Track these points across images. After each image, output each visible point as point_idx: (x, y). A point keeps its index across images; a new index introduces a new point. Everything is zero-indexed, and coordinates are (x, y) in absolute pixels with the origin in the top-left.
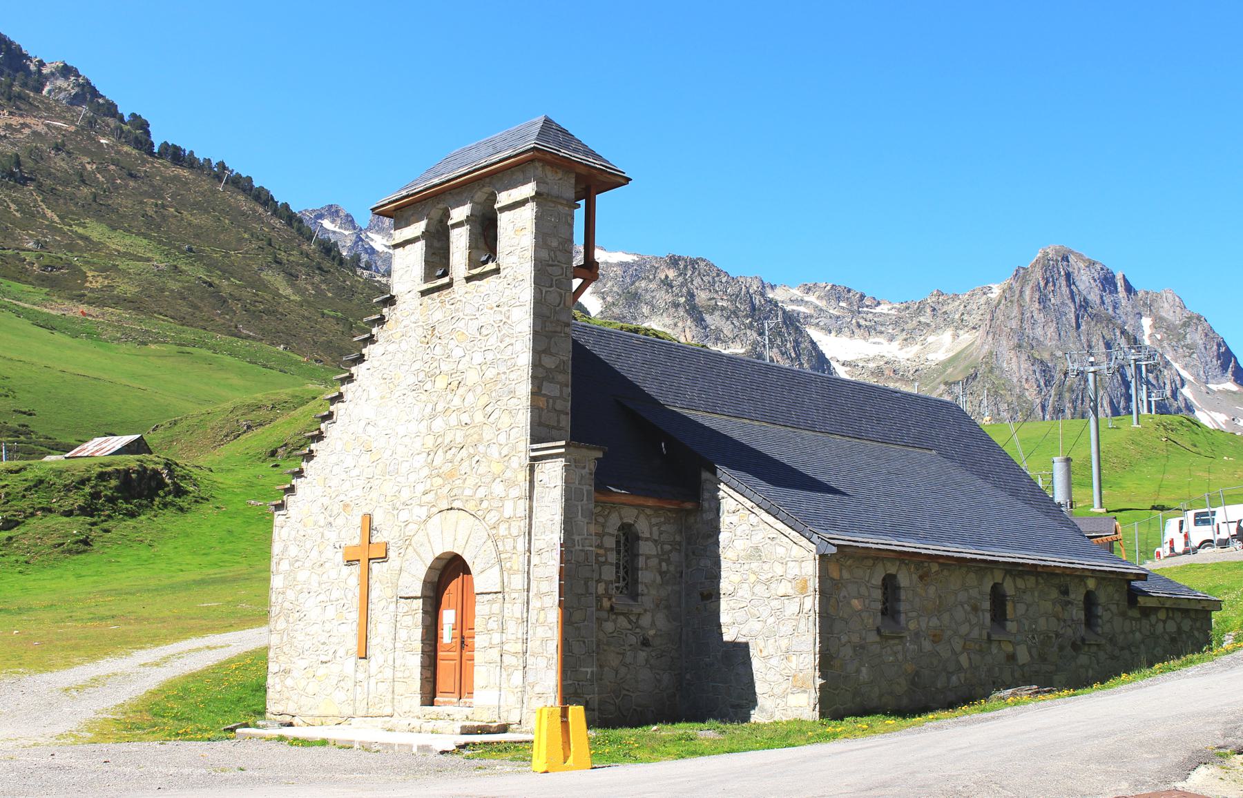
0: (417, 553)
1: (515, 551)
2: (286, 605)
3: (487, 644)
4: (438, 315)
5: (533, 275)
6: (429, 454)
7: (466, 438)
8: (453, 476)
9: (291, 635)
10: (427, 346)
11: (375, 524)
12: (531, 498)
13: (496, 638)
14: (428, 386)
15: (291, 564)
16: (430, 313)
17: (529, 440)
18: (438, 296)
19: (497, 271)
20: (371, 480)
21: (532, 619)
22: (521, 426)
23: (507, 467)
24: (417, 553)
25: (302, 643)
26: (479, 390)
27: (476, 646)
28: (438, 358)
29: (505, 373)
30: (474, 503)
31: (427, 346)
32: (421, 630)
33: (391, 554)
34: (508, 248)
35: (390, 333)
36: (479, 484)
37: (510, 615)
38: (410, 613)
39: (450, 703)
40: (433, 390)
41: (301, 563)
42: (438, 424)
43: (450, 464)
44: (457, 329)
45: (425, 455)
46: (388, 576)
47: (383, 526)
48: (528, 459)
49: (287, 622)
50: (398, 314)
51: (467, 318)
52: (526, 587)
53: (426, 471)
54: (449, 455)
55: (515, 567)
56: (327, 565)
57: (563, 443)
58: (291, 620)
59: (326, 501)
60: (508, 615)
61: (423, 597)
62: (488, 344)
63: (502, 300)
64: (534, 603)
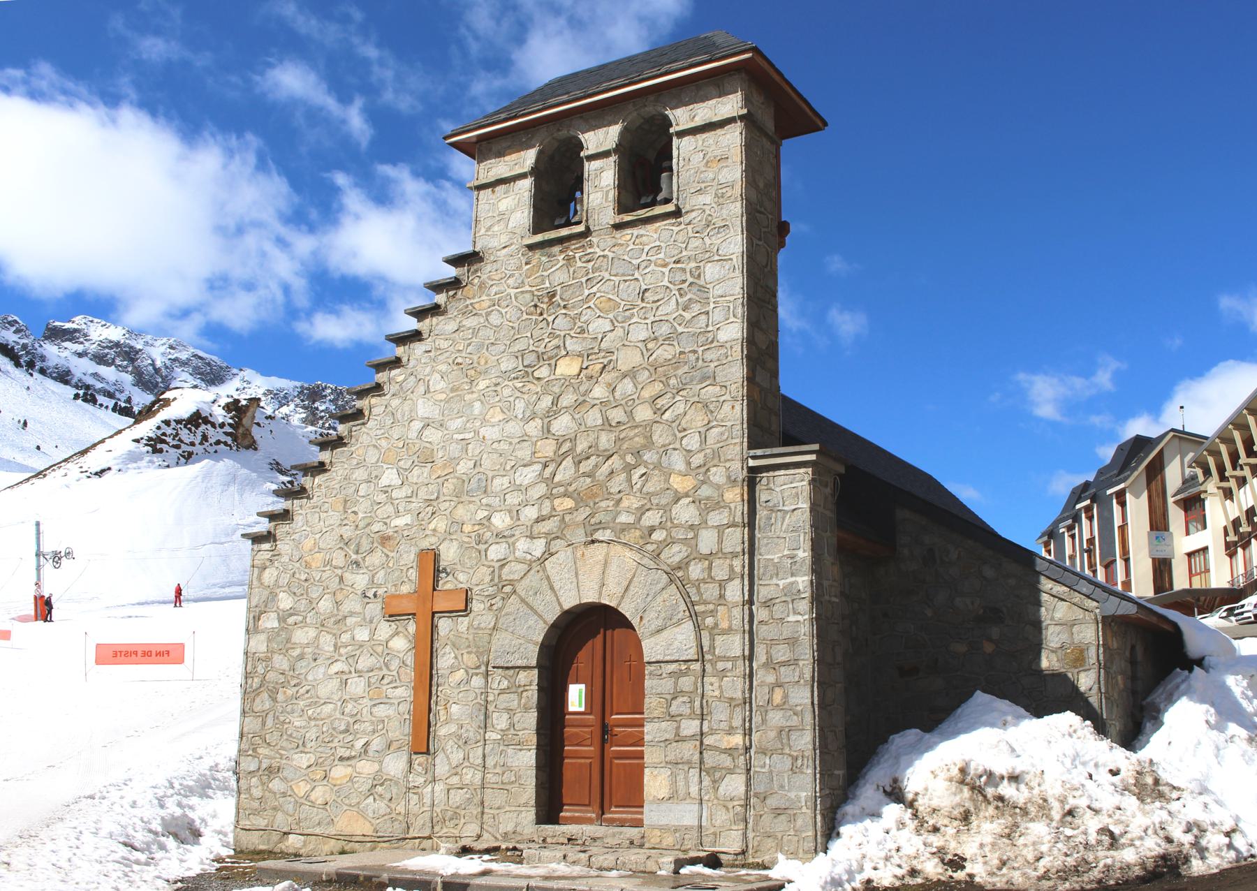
0: (527, 604)
1: (722, 601)
2: (271, 676)
3: (670, 736)
4: (560, 276)
5: (744, 218)
6: (545, 466)
7: (618, 443)
8: (594, 495)
9: (282, 719)
10: (541, 318)
11: (443, 564)
12: (751, 524)
13: (690, 727)
14: (543, 372)
15: (282, 619)
16: (545, 274)
17: (745, 444)
18: (561, 252)
19: (677, 213)
20: (435, 503)
21: (760, 696)
22: (729, 424)
23: (703, 482)
24: (527, 604)
25: (303, 731)
26: (643, 376)
27: (647, 738)
28: (562, 334)
29: (695, 352)
30: (638, 533)
31: (541, 318)
32: (536, 714)
33: (476, 606)
34: (695, 184)
35: (468, 302)
36: (647, 507)
37: (717, 693)
38: (514, 690)
39: (589, 821)
40: (553, 377)
41: (300, 618)
42: (562, 424)
43: (588, 480)
44: (598, 295)
45: (538, 467)
46: (471, 637)
47: (459, 567)
48: (745, 470)
49: (275, 700)
50: (484, 277)
51: (616, 279)
52: (747, 653)
53: (541, 489)
54: (586, 466)
55: (724, 625)
56: (350, 621)
57: (816, 447)
58: (280, 697)
59: (347, 532)
60: (710, 693)
61: (539, 666)
62: (659, 313)
63: (684, 253)
64: (764, 677)
